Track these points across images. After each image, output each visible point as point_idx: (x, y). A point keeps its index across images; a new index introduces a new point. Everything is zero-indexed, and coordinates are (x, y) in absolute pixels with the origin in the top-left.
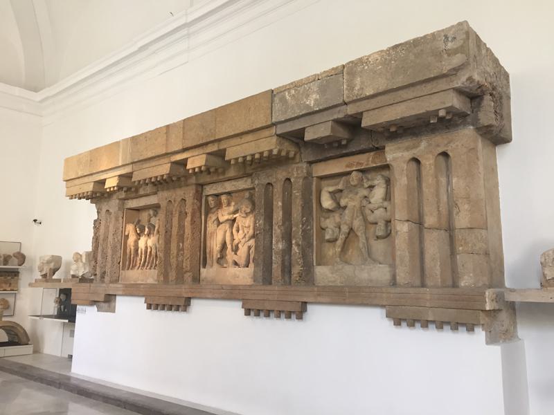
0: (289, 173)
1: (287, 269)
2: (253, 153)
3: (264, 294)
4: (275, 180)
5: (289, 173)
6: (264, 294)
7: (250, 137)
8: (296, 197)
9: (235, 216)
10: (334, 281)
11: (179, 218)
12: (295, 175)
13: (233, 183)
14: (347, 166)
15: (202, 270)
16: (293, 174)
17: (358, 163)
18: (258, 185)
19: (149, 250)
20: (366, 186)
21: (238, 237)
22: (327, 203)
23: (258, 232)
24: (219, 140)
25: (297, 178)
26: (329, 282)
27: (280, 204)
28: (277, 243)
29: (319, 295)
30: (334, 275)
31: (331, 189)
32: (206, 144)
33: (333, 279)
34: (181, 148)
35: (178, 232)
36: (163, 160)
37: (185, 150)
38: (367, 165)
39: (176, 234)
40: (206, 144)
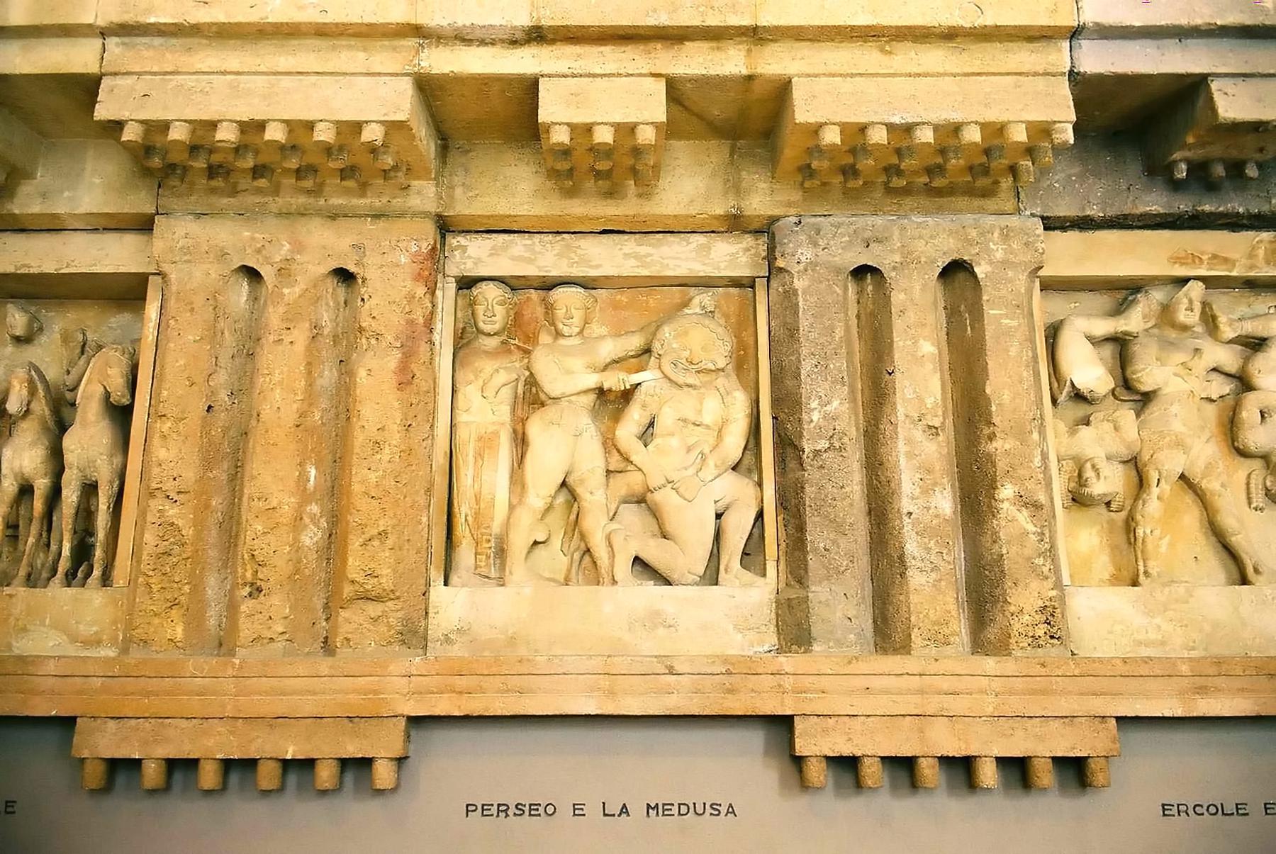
0: (970, 242)
1: (983, 592)
2: (956, 117)
3: (921, 692)
4: (898, 258)
5: (970, 242)
6: (921, 692)
7: (934, 57)
8: (1008, 333)
9: (636, 378)
10: (1163, 643)
11: (308, 349)
12: (999, 255)
13: (629, 244)
14: (1176, 260)
15: (438, 592)
16: (989, 251)
17: (1215, 257)
18: (813, 265)
19: (70, 496)
20: (1228, 333)
21: (658, 463)
22: (1088, 370)
23: (823, 444)
24: (755, 35)
25: (1005, 264)
26: (1140, 643)
27: (928, 348)
28: (927, 491)
29: (1202, 690)
30: (1158, 620)
31: (1104, 327)
32: (674, 36)
33: (1153, 635)
34: (523, 20)
35: (302, 415)
36: (312, 56)
37: (537, 35)
38: (1252, 267)
39: (290, 414)
40: (674, 36)
